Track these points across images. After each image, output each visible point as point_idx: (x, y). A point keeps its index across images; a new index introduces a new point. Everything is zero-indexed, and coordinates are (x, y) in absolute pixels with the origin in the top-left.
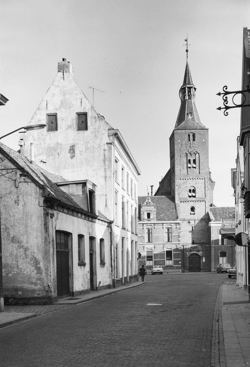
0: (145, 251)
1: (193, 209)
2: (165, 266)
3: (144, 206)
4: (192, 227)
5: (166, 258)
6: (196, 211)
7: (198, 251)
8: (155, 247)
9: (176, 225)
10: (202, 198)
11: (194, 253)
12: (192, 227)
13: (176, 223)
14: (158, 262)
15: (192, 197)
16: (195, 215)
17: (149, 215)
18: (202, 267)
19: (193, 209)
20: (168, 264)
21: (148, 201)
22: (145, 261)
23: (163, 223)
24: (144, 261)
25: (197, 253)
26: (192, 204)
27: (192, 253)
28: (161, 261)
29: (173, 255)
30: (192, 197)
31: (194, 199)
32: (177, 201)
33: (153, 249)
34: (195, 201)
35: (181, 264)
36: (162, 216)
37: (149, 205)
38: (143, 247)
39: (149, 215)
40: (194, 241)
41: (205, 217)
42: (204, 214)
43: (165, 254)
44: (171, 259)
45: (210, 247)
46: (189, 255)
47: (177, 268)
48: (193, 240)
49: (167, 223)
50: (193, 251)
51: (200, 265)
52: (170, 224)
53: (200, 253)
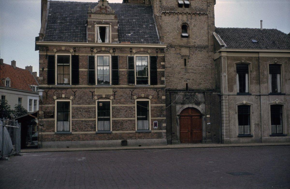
0: (95, 102)
1: (185, 28)
2: (134, 132)
3: (95, 13)
4: (185, 60)
5: (137, 115)
6: (190, 31)
7: (198, 104)
8: (115, 94)
9: (157, 52)
10: (202, 10)
11: (188, 108)
12: (185, 60)
13: (157, 49)
14: (122, 123)
15: (184, 7)
16: (190, 40)
17: (103, 31)
18: (204, 134)
19: (185, 28)
20: (141, 127)
21: (103, 5)
22: (95, 121)
23: (131, 48)
24: (92, 121)
25: (196, 107)
26: (184, 18)
27: (186, 106)
28: (126, 121)
29: (151, 111)
30: (184, 7)
31: (187, 10)
32: (157, 12)
33: (112, 97)
34: (190, 14)
35: (166, 128)
36: (130, 35)
37: (104, 11)
38: (91, 94)
39: (103, 31)
40: (189, 85)
41: (207, 44)
42: (205, 38)
43: (134, 107)
44: (146, 119)
45: (220, 96)
46: (180, 111)
47: (159, 136)
48: (187, 84)
49: (140, 48)
50: (188, 104)
51: (201, 130)
52: (146, 50)
53: (201, 108)
